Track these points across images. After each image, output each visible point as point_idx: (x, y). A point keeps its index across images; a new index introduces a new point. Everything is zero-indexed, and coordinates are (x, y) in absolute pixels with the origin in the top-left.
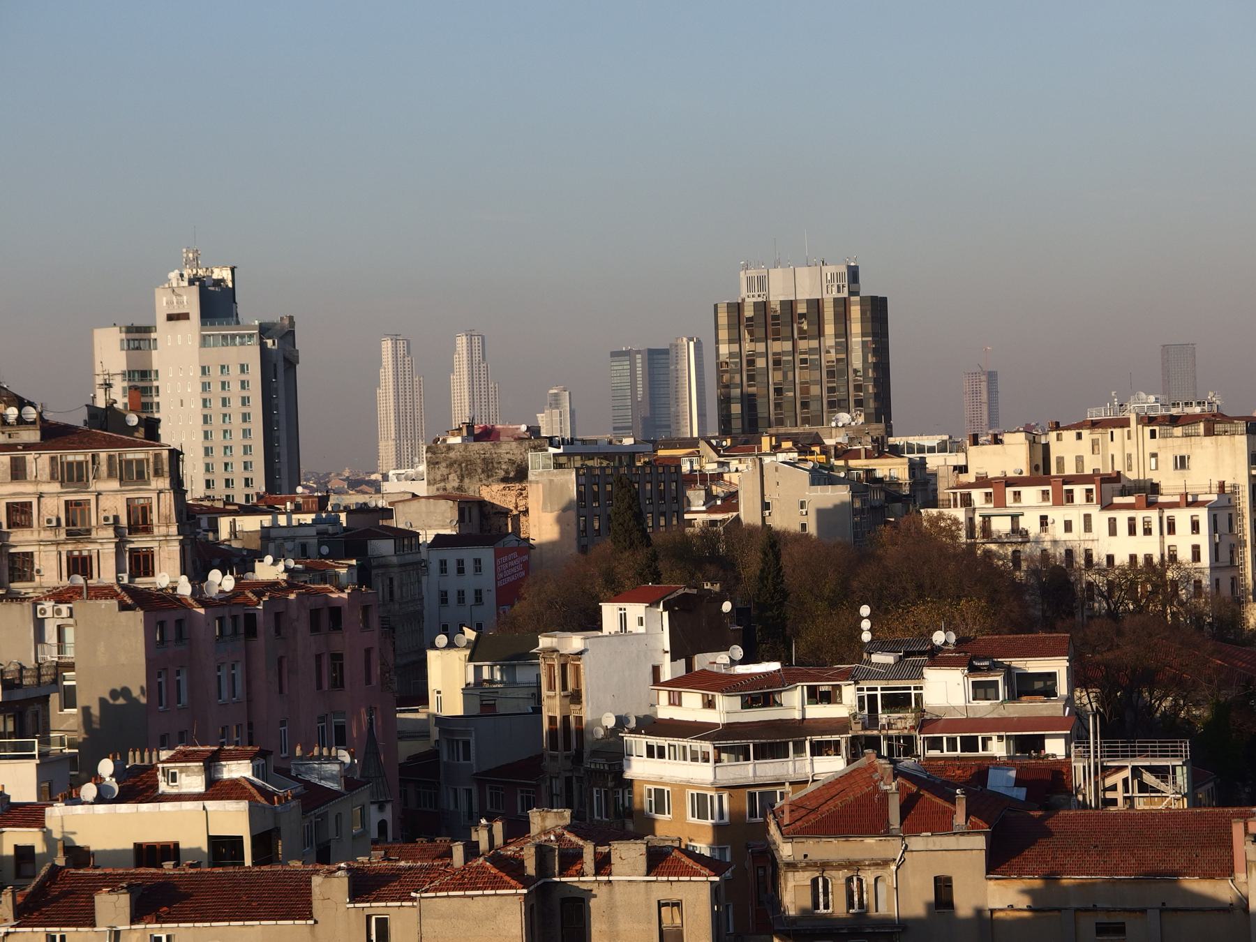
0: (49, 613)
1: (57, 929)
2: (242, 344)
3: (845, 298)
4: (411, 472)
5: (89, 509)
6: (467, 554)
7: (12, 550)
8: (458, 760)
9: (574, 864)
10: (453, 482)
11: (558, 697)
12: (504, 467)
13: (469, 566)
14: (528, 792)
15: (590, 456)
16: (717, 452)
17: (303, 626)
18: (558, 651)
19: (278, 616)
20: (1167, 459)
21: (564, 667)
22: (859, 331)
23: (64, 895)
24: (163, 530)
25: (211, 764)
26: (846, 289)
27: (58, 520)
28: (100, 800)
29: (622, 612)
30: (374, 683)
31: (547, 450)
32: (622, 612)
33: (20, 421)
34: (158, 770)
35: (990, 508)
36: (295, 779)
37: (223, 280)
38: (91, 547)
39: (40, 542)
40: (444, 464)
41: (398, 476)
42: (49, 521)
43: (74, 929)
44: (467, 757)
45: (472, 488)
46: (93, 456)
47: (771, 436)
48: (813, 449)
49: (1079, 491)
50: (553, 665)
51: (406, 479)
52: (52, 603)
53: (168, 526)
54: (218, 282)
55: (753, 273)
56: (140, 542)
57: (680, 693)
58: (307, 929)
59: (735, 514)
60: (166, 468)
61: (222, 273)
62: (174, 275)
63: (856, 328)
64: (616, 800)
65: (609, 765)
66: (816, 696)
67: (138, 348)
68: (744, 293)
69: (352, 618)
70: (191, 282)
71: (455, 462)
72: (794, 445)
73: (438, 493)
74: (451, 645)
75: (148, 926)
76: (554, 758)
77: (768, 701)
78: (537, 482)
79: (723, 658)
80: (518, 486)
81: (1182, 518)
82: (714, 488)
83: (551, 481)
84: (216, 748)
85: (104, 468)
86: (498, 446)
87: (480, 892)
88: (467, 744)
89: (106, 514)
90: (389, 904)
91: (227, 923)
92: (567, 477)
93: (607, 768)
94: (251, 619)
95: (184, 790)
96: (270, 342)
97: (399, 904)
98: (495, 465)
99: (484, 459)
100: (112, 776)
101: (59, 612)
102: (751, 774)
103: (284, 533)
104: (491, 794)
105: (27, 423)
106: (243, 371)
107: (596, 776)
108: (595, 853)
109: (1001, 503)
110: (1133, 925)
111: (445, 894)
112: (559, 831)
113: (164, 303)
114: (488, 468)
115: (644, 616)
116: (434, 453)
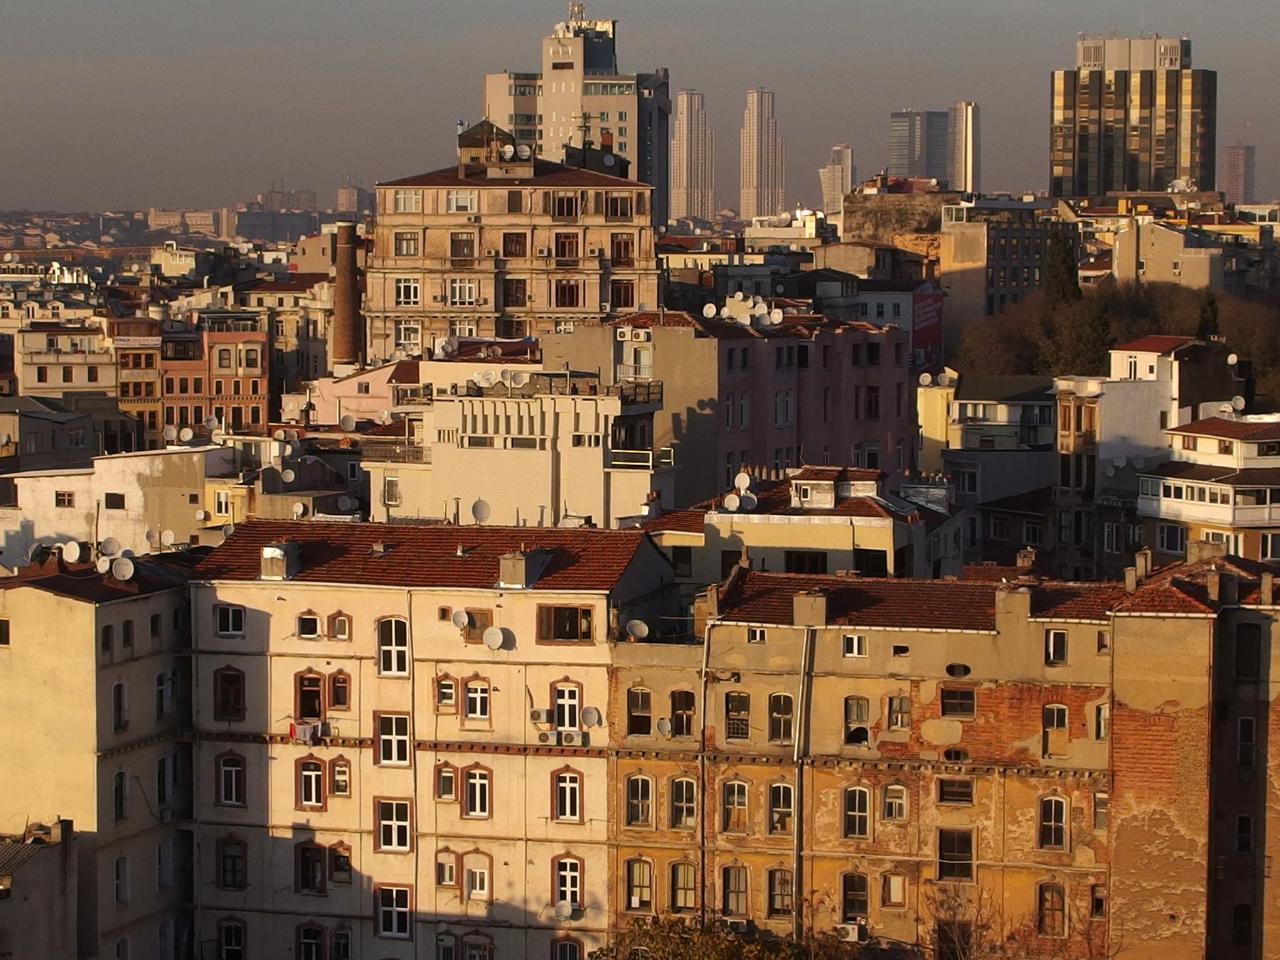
0: (628, 337)
1: (759, 625)
2: (622, 93)
3: (1177, 71)
4: (774, 219)
5: (577, 243)
6: (888, 299)
7: (508, 277)
8: (963, 490)
9: (1251, 593)
10: (869, 230)
11: (1072, 437)
12: (917, 218)
13: (888, 309)
14: (1034, 523)
15: (993, 212)
16: (1075, 212)
17: (847, 360)
18: (1074, 393)
19: (825, 347)
21: (1079, 410)
22: (1190, 102)
23: (760, 594)
24: (643, 264)
25: (841, 481)
26: (1178, 63)
27: (549, 250)
28: (741, 510)
29: (1132, 360)
30: (903, 415)
31: (959, 204)
32: (1132, 360)
33: (516, 158)
34: (791, 486)
36: (904, 499)
37: (605, 33)
38: (577, 277)
39: (532, 271)
40: (860, 214)
41: (761, 222)
42: (541, 252)
43: (775, 626)
44: (972, 488)
45: (886, 237)
46: (582, 193)
47: (1127, 199)
48: (1168, 213)
50: (1069, 407)
51: (770, 225)
52: (631, 328)
53: (647, 261)
54: (602, 34)
55: (1090, 43)
56: (621, 275)
57: (1195, 439)
58: (990, 639)
59: (1108, 271)
60: (648, 207)
61: (604, 26)
62: (560, 27)
63: (1186, 100)
64: (1127, 535)
65: (1123, 503)
67: (523, 94)
68: (1080, 62)
69: (887, 354)
70: (576, 34)
71: (871, 211)
72: (1149, 208)
73: (854, 240)
74: (935, 383)
75: (843, 627)
76: (1064, 493)
78: (950, 234)
79: (1227, 407)
80: (930, 236)
82: (1088, 246)
83: (963, 234)
84: (841, 469)
85: (591, 204)
86: (913, 198)
87: (1171, 615)
88: (973, 477)
89: (592, 247)
90: (1069, 620)
91: (915, 629)
92: (980, 230)
93: (1120, 504)
94: (803, 350)
95: (815, 506)
96: (646, 92)
97: (1077, 621)
98: (909, 216)
99: (899, 210)
100: (748, 489)
101: (637, 336)
102: (1267, 517)
103: (741, 272)
104: (995, 524)
105: (521, 160)
106: (621, 118)
108: (1274, 585)
111: (1138, 614)
112: (1219, 562)
113: (550, 53)
114: (902, 220)
115: (1155, 364)
116: (851, 202)
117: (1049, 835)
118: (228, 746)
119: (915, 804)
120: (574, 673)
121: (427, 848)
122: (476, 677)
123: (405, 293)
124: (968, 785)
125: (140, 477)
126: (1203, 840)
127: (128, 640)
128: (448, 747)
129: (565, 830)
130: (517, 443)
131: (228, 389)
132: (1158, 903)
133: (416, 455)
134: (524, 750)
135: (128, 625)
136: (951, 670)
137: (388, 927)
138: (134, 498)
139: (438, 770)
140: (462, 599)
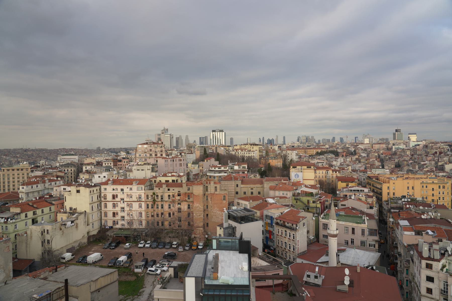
10: (189, 148)
20: (251, 147)
35: (236, 152)
49: (244, 150)
66: (224, 168)
77: (220, 168)
81: (253, 153)
107: (204, 175)
109: (237, 151)
110: (254, 188)
117: (189, 208)
118: (105, 202)
119: (175, 205)
120: (141, 194)
121: (126, 212)
122: (131, 194)
123: (140, 155)
124: (180, 203)
125: (107, 174)
126: (202, 208)
127: (93, 192)
128: (128, 201)
129: (140, 209)
130: (142, 170)
131: (125, 165)
132: (198, 214)
133: (132, 171)
134: (136, 202)
135: (93, 190)
136: (178, 192)
137: (122, 220)
138: (106, 176)
139: (127, 204)
140: (130, 186)
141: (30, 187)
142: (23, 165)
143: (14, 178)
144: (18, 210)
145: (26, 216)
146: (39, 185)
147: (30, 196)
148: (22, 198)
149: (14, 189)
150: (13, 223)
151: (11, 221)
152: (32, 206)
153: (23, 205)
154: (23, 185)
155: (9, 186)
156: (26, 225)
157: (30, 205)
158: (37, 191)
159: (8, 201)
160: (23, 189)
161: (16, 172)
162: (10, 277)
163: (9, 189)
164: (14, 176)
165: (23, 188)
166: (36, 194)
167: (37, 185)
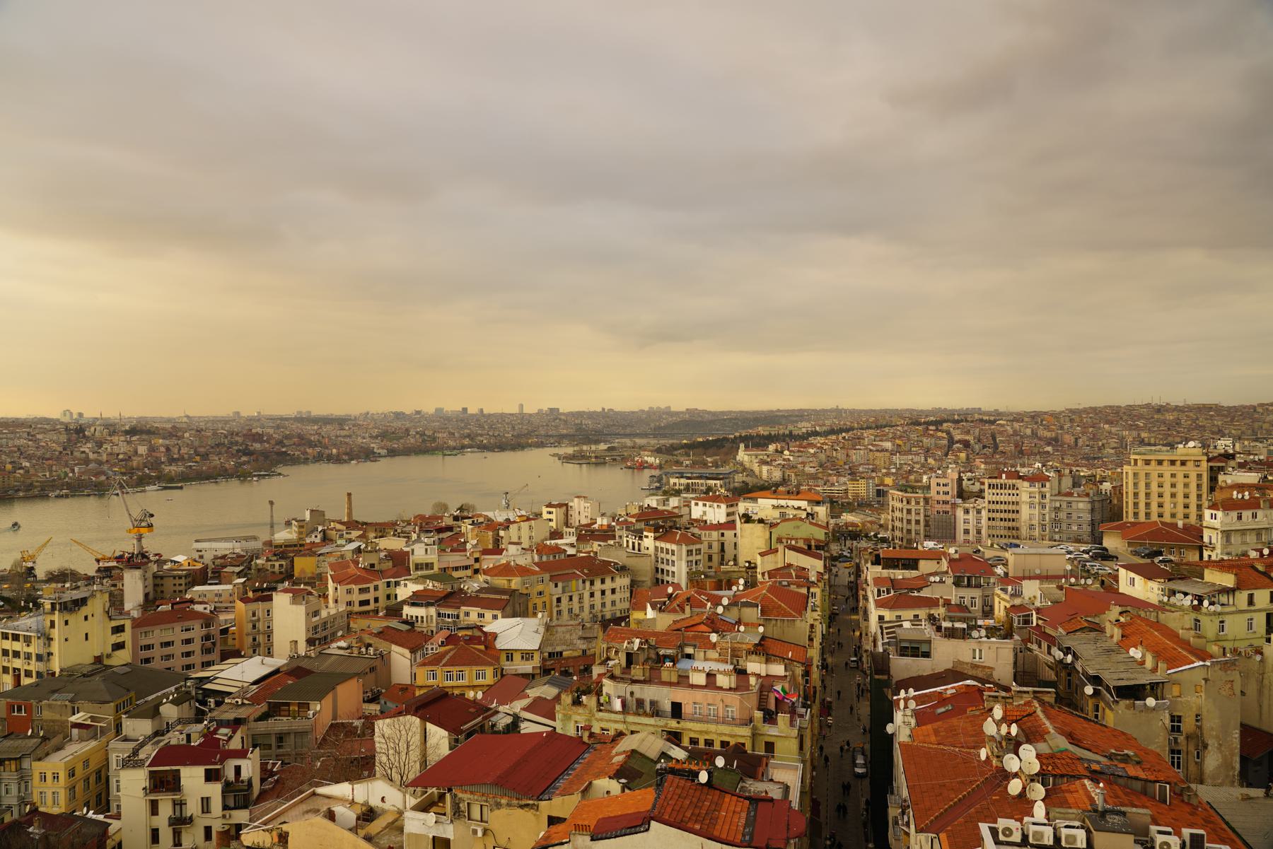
141: (1234, 514)
142: (1185, 451)
143: (1160, 486)
144: (1228, 580)
145: (1251, 601)
146: (1260, 513)
147: (1233, 541)
148: (1211, 544)
149: (1161, 516)
150: (1215, 613)
151: (1212, 608)
152: (1265, 574)
153: (1238, 567)
154: (1213, 506)
155: (1148, 505)
156: (1250, 626)
157: (1257, 570)
158: (1254, 529)
159: (1163, 545)
160: (1213, 521)
161: (1167, 470)
162: (1233, 768)
163: (1148, 515)
164: (1161, 479)
165: (1213, 517)
166: (1251, 538)
167: (1254, 511)
